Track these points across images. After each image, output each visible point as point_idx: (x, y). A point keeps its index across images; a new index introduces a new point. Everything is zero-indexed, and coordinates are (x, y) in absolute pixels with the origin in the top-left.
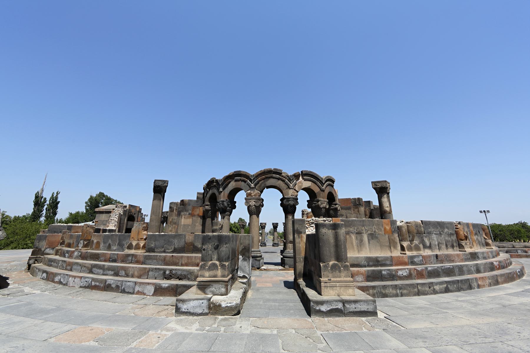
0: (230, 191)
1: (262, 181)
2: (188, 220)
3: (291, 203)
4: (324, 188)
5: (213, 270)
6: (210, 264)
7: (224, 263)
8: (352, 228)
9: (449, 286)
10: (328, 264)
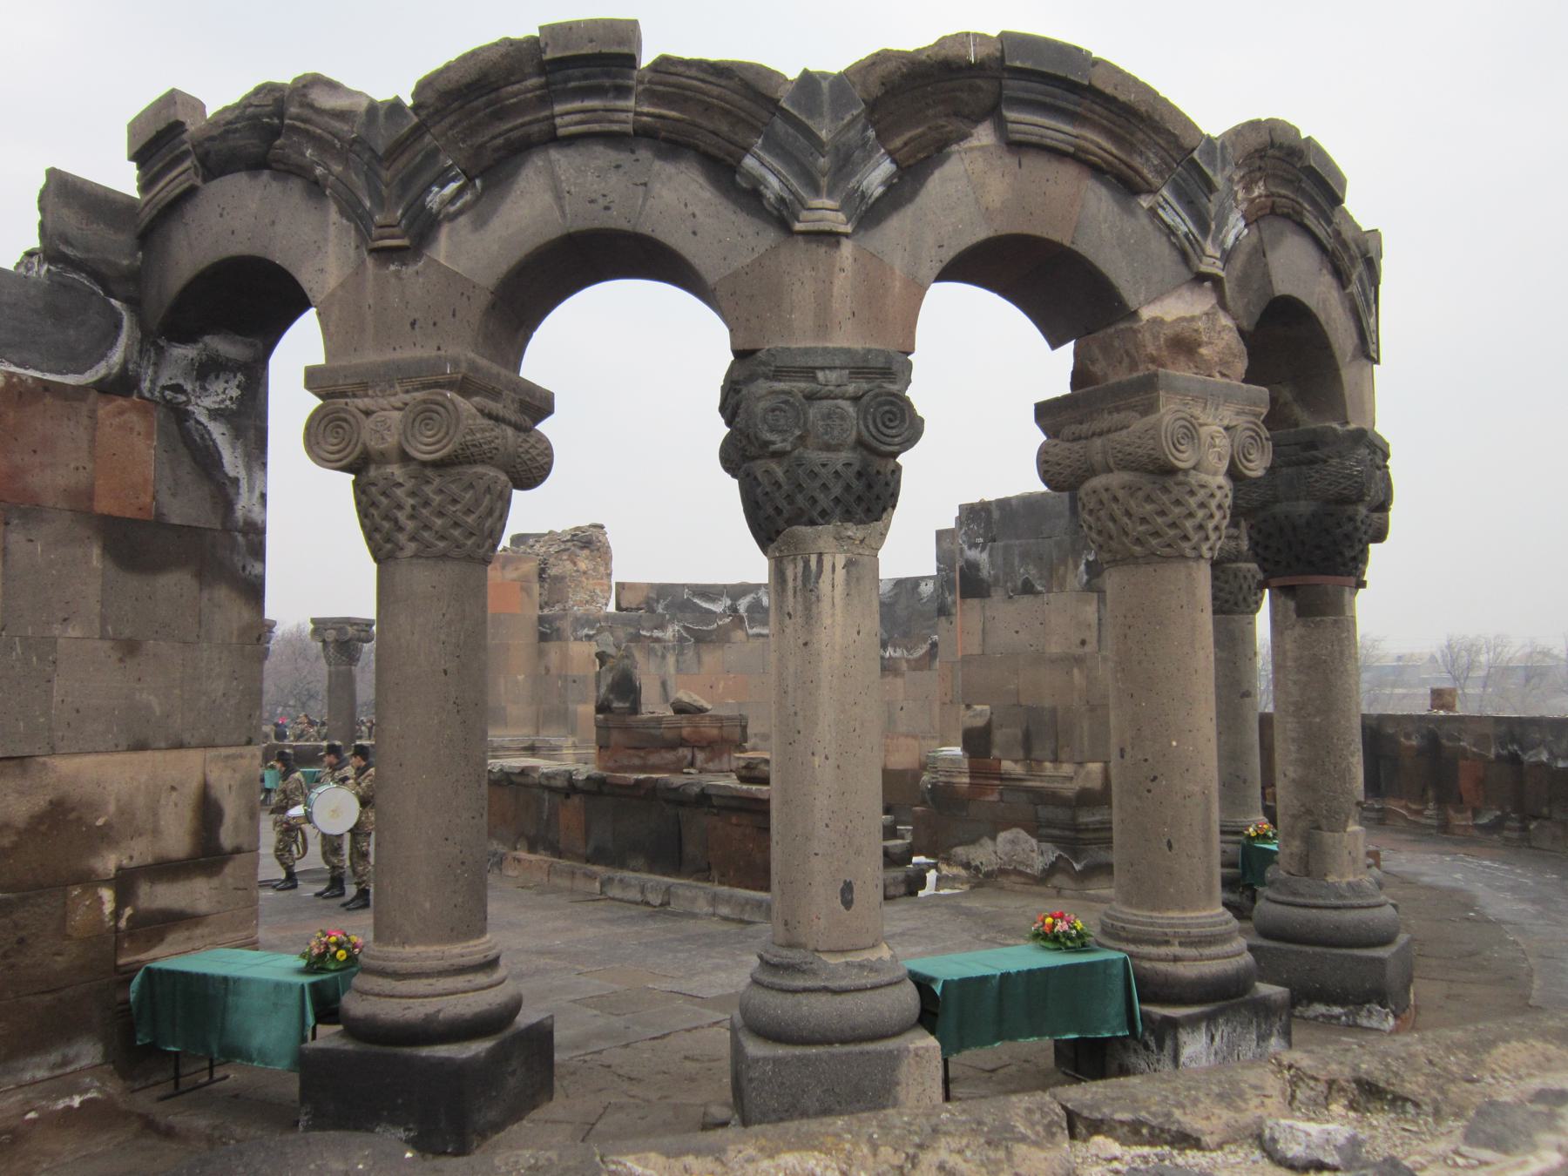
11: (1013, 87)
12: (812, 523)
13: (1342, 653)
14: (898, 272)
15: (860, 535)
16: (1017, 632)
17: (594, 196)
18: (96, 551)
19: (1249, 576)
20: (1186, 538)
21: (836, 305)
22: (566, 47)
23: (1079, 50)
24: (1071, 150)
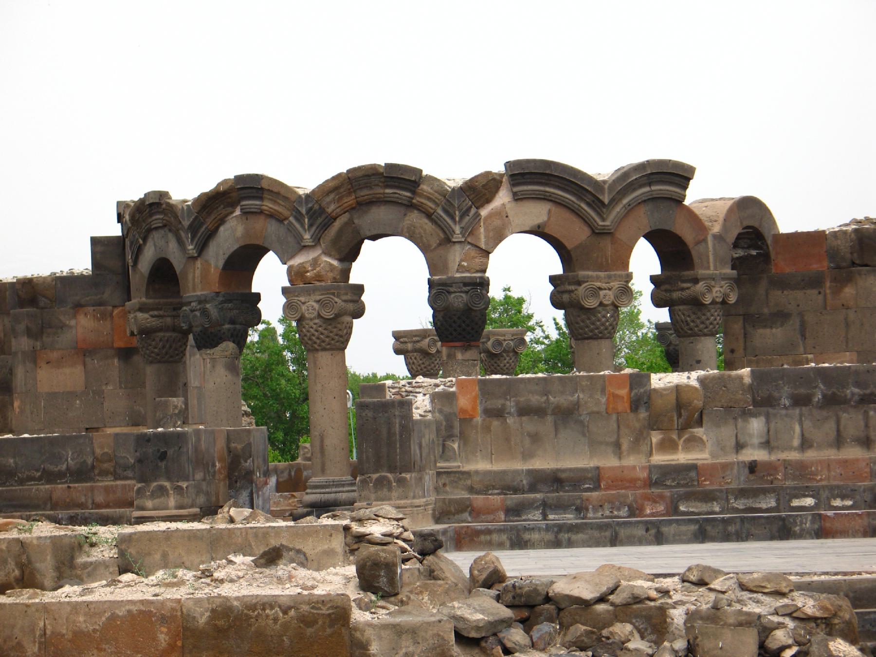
0: (227, 256)
1: (344, 218)
2: (67, 370)
3: (458, 300)
4: (607, 223)
5: (160, 497)
6: (154, 487)
7: (179, 484)
8: (510, 402)
9: (709, 528)
10: (370, 477)
14: (212, 266)
15: (212, 352)
18: (116, 361)
19: (680, 313)
21: (196, 280)
23: (257, 175)
24: (259, 211)
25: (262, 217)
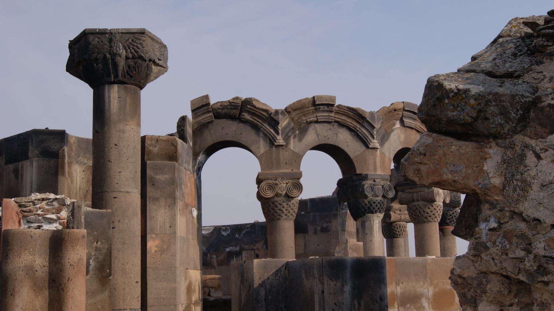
11: (405, 113)
12: (373, 213)
13: (454, 246)
16: (318, 245)
17: (326, 136)
19: (403, 226)
20: (436, 217)
22: (321, 102)
25: (414, 132)
